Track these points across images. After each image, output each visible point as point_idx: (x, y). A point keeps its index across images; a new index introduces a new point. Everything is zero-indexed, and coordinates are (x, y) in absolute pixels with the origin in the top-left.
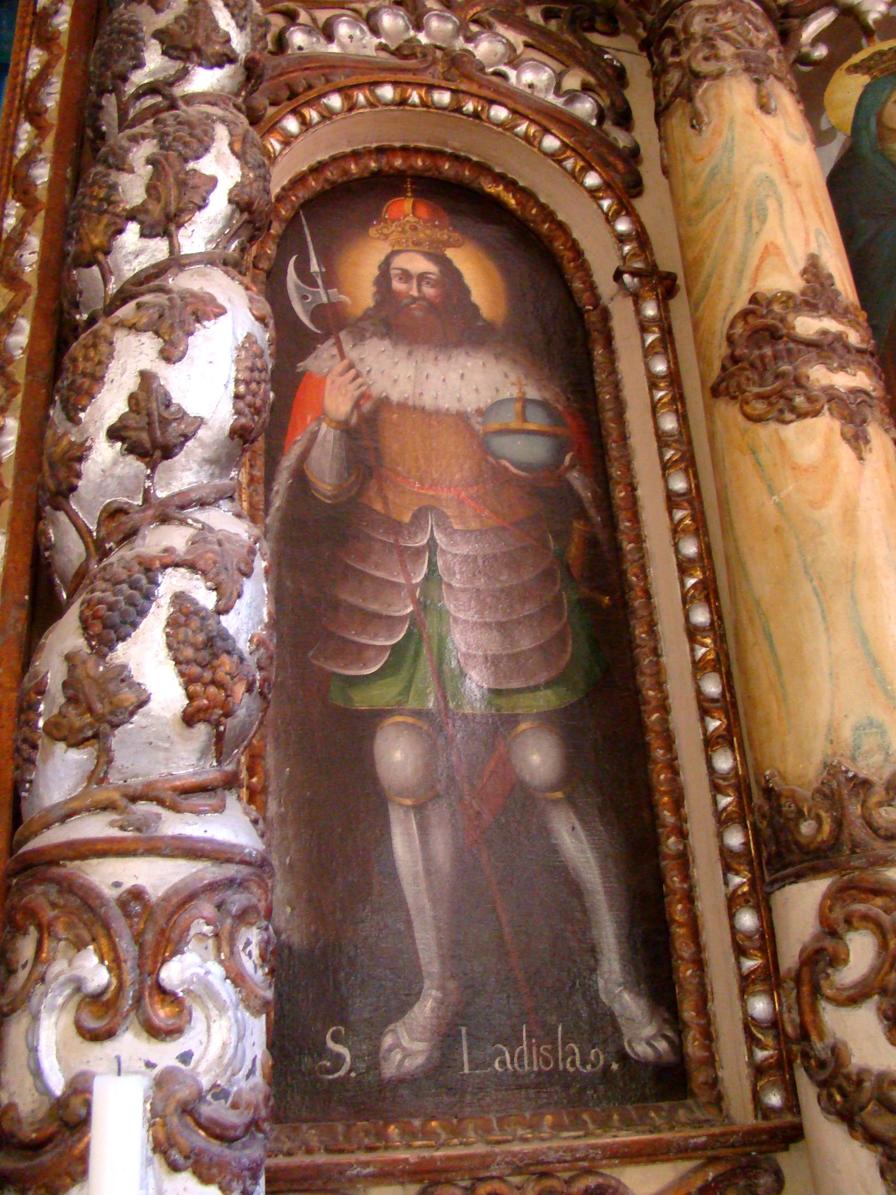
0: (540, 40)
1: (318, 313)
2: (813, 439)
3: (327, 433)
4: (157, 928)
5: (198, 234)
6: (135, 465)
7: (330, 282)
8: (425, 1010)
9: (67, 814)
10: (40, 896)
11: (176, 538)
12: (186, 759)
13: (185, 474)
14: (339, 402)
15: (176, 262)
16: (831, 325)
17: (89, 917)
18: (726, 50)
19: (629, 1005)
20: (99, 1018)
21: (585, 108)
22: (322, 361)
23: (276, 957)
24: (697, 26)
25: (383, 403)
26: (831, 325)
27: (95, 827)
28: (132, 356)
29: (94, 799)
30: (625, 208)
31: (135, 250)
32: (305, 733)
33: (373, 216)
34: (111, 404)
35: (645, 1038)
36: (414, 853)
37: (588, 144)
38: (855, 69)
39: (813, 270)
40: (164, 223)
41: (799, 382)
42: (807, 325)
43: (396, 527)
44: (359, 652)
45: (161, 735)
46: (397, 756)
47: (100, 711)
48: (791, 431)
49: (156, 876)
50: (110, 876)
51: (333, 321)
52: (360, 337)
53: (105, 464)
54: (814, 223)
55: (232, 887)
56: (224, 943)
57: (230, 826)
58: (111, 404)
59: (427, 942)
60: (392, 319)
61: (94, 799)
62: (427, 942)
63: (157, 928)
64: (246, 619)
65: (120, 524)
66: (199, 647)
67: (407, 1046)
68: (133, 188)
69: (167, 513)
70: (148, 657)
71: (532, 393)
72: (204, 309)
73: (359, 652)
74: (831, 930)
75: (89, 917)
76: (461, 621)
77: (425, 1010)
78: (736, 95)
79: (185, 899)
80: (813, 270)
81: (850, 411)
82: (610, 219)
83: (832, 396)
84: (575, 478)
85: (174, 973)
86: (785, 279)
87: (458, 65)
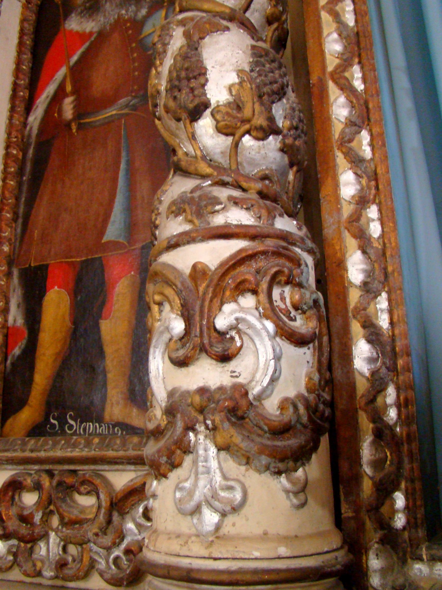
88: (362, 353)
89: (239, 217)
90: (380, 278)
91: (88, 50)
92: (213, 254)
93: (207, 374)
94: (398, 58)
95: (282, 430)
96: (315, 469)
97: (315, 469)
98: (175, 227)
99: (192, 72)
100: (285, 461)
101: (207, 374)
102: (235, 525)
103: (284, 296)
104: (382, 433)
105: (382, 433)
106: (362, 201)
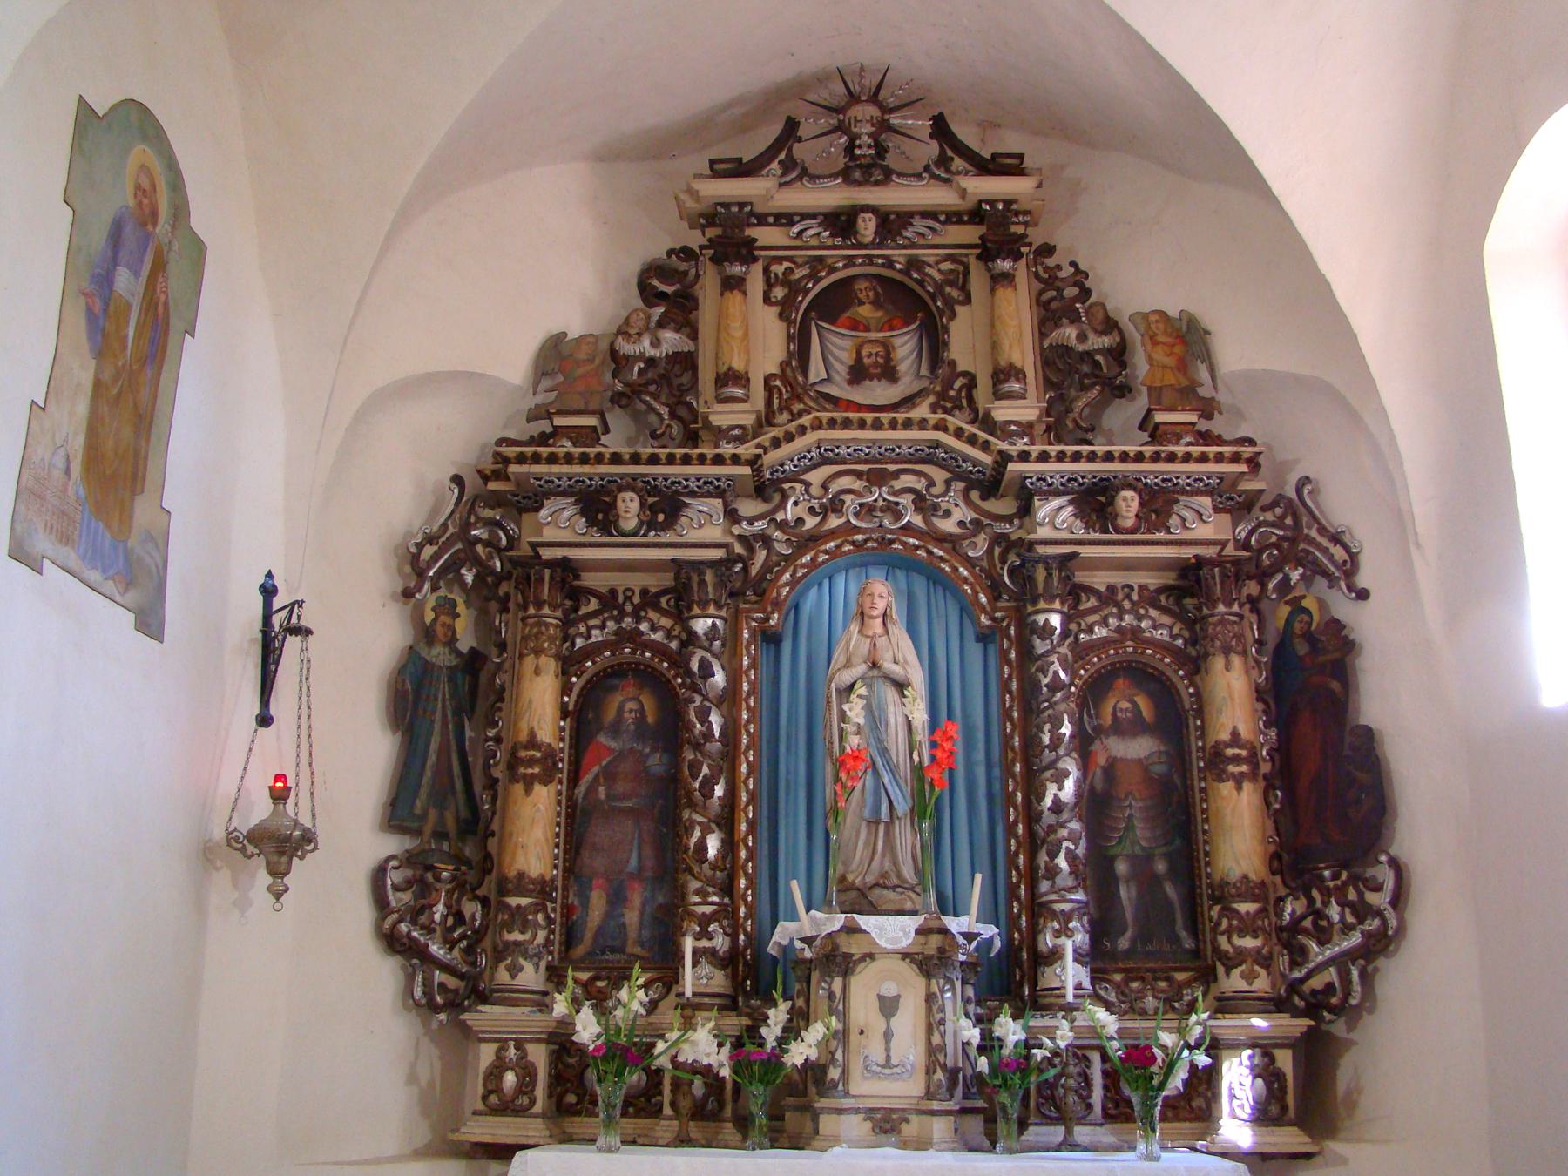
0: (1165, 610)
1: (1094, 729)
2: (1227, 788)
3: (1099, 771)
4: (1067, 917)
5: (1061, 752)
6: (1054, 817)
7: (1098, 716)
8: (1129, 934)
9: (1046, 894)
10: (1044, 910)
11: (1064, 833)
12: (1070, 882)
13: (1065, 816)
14: (1102, 760)
15: (1058, 758)
16: (1237, 751)
17: (1054, 915)
18: (1218, 643)
19: (1184, 934)
20: (1057, 934)
21: (1180, 642)
22: (1096, 746)
23: (1090, 922)
24: (1210, 631)
25: (1115, 758)
26: (1237, 751)
27: (1053, 897)
28: (1052, 789)
29: (1053, 890)
30: (1191, 685)
31: (1048, 756)
32: (1097, 871)
33: (1110, 688)
34: (1048, 801)
35: (1188, 944)
36: (1126, 893)
37: (1180, 657)
38: (1287, 603)
39: (1235, 734)
40: (1054, 745)
41: (1224, 771)
42: (1229, 752)
43: (1120, 800)
44: (1110, 839)
45: (1065, 880)
46: (1121, 867)
47: (1053, 872)
48: (1222, 785)
49: (1066, 907)
50: (1058, 907)
51: (1099, 731)
52: (1107, 736)
53: (1048, 818)
54: (1238, 713)
55: (1082, 908)
56: (1080, 920)
57: (1079, 896)
58: (1048, 801)
59: (1129, 915)
60: (1119, 728)
61: (1053, 890)
62: (1129, 915)
63: (1067, 917)
64: (1081, 851)
65: (1052, 829)
66: (1071, 858)
67: (1124, 943)
68: (1046, 739)
69: (1063, 825)
70: (1062, 862)
71: (1162, 748)
72: (1066, 774)
73: (1110, 839)
74: (1220, 919)
75: (1054, 915)
76: (1137, 828)
77: (1129, 934)
78: (1218, 663)
79: (1072, 911)
80: (1235, 734)
81: (1238, 780)
82: (1187, 687)
83: (1233, 774)
84: (1177, 780)
85: (1071, 925)
86: (1225, 736)
87: (1135, 633)
88: (742, 937)
89: (715, 899)
90: (749, 915)
91: (614, 759)
92: (708, 909)
93: (705, 943)
94: (765, 834)
95: (723, 959)
96: (729, 971)
97: (729, 971)
98: (697, 899)
99: (702, 846)
100: (723, 968)
101: (705, 943)
102: (712, 982)
103: (725, 922)
104: (746, 963)
105: (746, 963)
106: (747, 889)
